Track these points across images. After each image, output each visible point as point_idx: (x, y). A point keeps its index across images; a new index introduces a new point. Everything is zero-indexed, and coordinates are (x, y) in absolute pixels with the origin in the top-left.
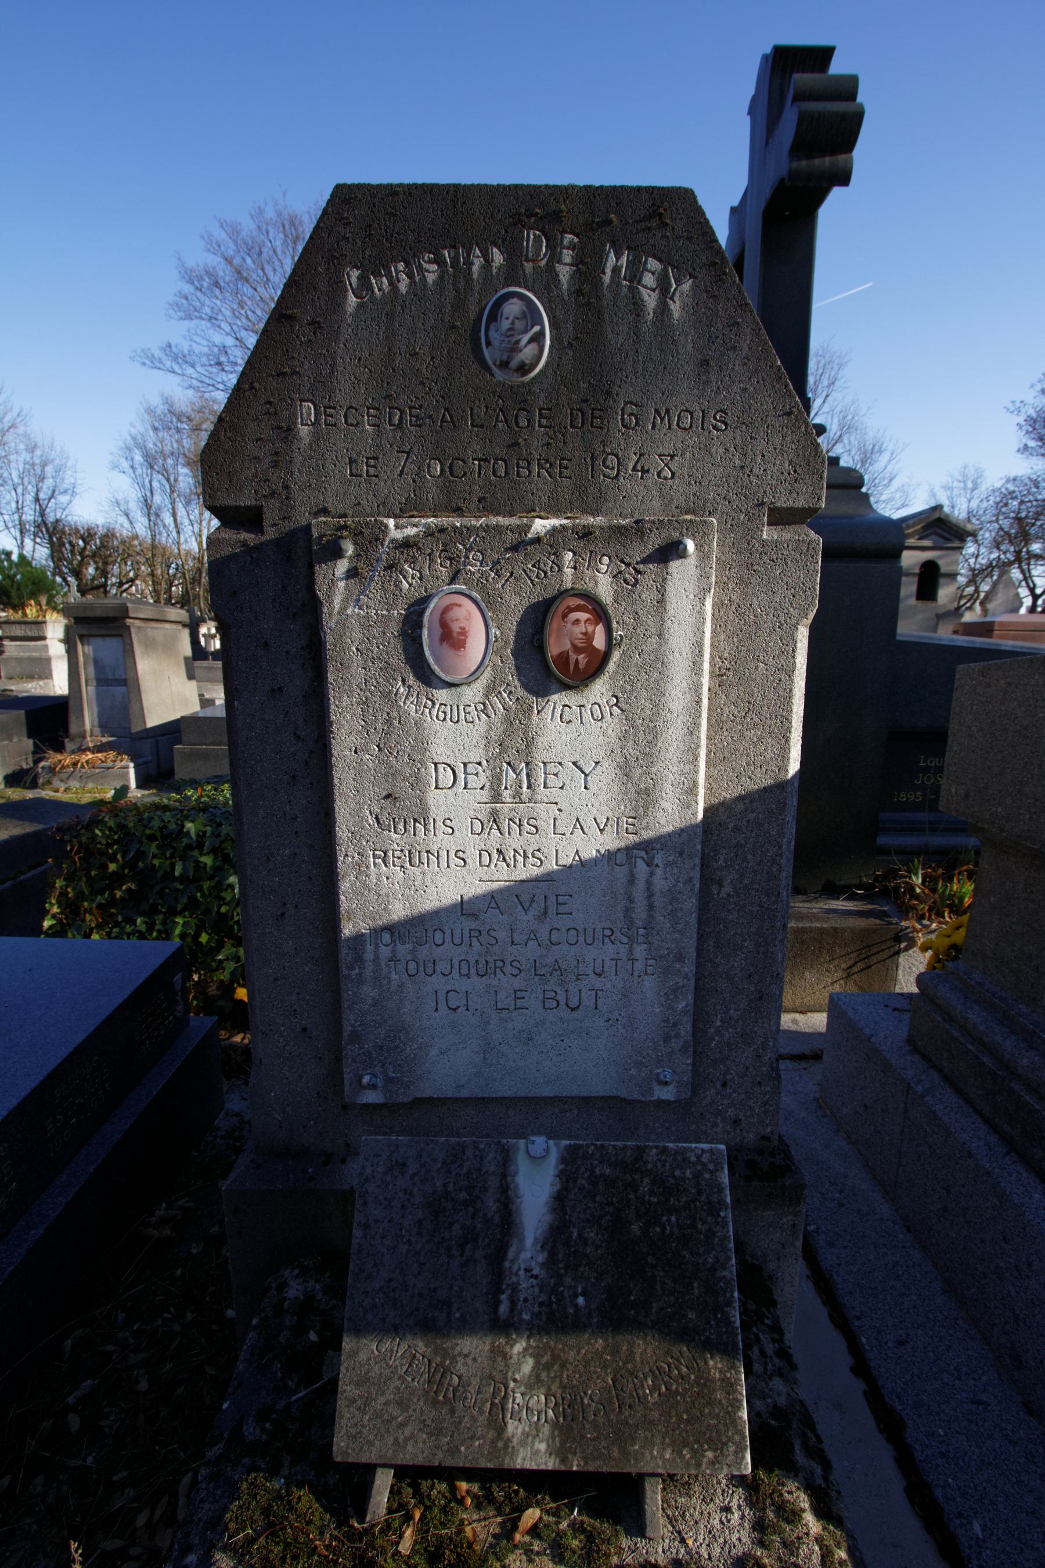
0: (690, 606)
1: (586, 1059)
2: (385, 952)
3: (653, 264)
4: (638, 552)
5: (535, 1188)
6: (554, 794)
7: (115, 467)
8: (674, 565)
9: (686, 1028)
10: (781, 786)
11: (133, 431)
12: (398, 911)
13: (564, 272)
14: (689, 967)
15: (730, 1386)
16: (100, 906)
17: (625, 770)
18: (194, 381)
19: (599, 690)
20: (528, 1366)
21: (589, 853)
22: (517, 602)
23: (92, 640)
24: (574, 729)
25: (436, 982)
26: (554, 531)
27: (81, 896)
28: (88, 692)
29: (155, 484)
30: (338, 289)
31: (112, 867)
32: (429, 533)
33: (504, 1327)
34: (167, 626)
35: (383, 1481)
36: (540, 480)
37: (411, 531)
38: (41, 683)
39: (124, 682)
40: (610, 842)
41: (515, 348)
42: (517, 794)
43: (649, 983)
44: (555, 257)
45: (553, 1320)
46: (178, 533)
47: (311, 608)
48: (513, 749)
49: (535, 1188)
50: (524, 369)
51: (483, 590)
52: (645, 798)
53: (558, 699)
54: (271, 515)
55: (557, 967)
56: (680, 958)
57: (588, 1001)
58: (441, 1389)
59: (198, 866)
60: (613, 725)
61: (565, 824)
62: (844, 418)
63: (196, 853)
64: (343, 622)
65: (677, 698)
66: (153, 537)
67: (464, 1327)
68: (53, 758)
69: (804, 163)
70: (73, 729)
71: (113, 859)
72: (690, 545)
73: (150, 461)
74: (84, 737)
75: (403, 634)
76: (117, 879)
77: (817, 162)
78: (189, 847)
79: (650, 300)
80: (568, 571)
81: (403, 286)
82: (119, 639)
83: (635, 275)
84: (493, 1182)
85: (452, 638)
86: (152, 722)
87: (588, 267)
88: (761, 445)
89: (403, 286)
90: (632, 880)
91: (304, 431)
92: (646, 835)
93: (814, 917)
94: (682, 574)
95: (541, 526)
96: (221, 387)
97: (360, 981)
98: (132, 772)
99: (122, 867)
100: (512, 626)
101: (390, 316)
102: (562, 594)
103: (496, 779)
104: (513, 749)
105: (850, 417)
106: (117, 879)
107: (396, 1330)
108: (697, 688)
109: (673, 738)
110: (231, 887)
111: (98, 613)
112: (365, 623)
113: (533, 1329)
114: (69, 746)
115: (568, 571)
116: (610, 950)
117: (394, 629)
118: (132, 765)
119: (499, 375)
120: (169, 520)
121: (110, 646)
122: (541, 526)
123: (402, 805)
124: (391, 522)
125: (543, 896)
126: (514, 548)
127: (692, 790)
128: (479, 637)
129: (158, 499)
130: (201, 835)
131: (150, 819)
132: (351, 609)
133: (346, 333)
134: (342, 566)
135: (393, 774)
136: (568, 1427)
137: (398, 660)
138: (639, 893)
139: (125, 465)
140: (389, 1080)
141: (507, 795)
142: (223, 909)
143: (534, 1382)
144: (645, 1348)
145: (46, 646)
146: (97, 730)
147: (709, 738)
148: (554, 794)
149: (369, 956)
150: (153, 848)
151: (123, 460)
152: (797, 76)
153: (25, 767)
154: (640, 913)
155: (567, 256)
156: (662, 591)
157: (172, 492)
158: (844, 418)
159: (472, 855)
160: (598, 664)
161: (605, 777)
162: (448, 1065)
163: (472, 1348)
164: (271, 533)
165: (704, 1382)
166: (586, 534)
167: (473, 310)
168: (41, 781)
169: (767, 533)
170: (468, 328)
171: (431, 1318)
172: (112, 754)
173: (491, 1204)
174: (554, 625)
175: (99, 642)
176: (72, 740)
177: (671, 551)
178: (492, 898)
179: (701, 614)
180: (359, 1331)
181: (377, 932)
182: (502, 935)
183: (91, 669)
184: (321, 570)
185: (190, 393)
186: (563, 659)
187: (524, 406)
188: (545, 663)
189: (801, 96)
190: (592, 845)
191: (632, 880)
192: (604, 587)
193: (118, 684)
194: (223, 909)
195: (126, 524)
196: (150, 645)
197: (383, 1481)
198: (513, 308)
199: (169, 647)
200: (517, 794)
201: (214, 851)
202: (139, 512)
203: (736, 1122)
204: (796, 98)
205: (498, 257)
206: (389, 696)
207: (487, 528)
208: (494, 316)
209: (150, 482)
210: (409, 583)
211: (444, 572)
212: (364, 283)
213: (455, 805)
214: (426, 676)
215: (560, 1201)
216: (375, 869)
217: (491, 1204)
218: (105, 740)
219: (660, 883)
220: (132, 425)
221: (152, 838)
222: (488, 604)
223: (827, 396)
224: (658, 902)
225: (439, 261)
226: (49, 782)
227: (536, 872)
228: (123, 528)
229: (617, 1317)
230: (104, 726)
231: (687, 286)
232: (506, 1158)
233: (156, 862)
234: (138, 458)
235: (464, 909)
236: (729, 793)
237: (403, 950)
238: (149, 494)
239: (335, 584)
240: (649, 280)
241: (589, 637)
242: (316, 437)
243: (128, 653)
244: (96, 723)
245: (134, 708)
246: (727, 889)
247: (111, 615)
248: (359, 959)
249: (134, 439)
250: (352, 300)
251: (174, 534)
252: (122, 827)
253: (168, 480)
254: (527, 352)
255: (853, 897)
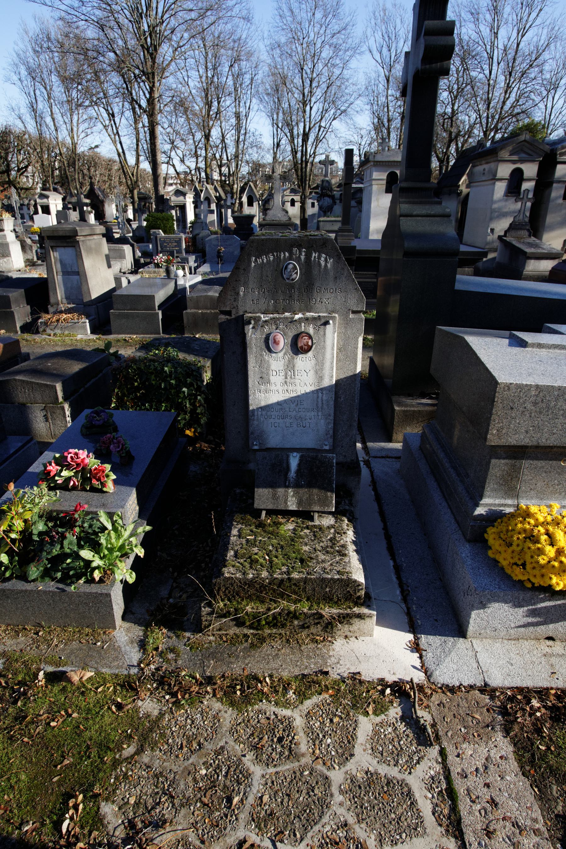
0: (332, 336)
1: (309, 440)
2: (260, 413)
3: (324, 255)
4: (319, 323)
5: (294, 462)
6: (300, 377)
7: (8, 79)
8: (327, 326)
9: (331, 432)
10: (355, 376)
11: (16, 48)
12: (263, 404)
13: (303, 257)
14: (332, 418)
15: (332, 497)
16: (132, 399)
17: (316, 372)
18: (63, 14)
19: (310, 354)
20: (292, 493)
21: (308, 391)
22: (291, 334)
23: (58, 249)
24: (304, 362)
25: (272, 420)
26: (300, 319)
27: (124, 395)
28: (58, 279)
29: (38, 92)
30: (250, 262)
31: (136, 384)
32: (271, 319)
33: (288, 487)
34: (95, 237)
35: (264, 513)
36: (297, 304)
37: (267, 318)
38: (5, 260)
39: (78, 273)
40: (313, 388)
41: (291, 275)
42: (291, 377)
43: (322, 421)
44: (300, 254)
45: (297, 485)
46: (56, 130)
47: (244, 335)
48: (290, 367)
49: (294, 462)
50: (293, 280)
51: (283, 332)
52: (321, 378)
53: (301, 356)
54: (234, 312)
55: (300, 417)
56: (330, 415)
57: (308, 425)
58: (275, 497)
59: (171, 384)
60: (313, 362)
61: (302, 384)
62: (553, 29)
63: (168, 379)
64: (251, 339)
65: (328, 355)
66: (40, 134)
67: (279, 487)
68: (45, 317)
69: (428, 66)
70: (52, 300)
71: (136, 381)
72: (331, 322)
73: (31, 72)
74: (58, 304)
75: (265, 341)
76: (138, 389)
77: (434, 65)
78: (167, 377)
79: (323, 263)
80: (303, 327)
81: (265, 261)
82: (73, 248)
83: (319, 258)
84: (285, 461)
85: (276, 342)
86: (94, 295)
87: (308, 256)
88: (349, 296)
89: (265, 261)
90: (318, 397)
91: (241, 293)
92: (321, 387)
93: (413, 406)
94: (329, 328)
95: (297, 317)
96: (83, 17)
97: (254, 420)
98: (88, 324)
99: (139, 384)
100: (290, 340)
101: (262, 268)
102: (302, 332)
103: (286, 374)
104: (290, 367)
105: (556, 28)
106: (138, 389)
107: (266, 487)
108: (333, 354)
109: (327, 365)
110: (184, 392)
111: (61, 234)
112: (256, 339)
113: (293, 487)
114: (51, 310)
115: (303, 327)
116: (313, 413)
117: (263, 340)
118: (87, 321)
119: (287, 281)
120: (48, 120)
121: (69, 252)
122: (297, 317)
123: (264, 379)
124: (262, 316)
125: (297, 401)
126: (291, 322)
127: (332, 377)
128: (283, 342)
129: (40, 106)
130: (171, 372)
131: (150, 366)
132: (253, 336)
133: (252, 272)
134: (251, 326)
135: (262, 372)
136: (300, 503)
137: (264, 347)
138: (320, 400)
139: (15, 78)
140: (260, 444)
141: (289, 377)
142: (180, 401)
143: (293, 496)
144: (315, 491)
145: (5, 235)
146: (65, 301)
147: (337, 364)
148: (300, 377)
149: (256, 414)
150: (153, 377)
151: (13, 74)
152: (426, 22)
153: (28, 321)
154: (320, 405)
155: (303, 254)
156: (325, 332)
157: (49, 98)
158: (553, 29)
159: (280, 391)
160: (309, 349)
161: (312, 373)
162: (274, 440)
163: (281, 491)
164: (233, 316)
165: (327, 497)
166: (307, 319)
167: (281, 266)
168: (41, 330)
169: (351, 316)
170: (280, 270)
171: (273, 485)
172: (76, 315)
173: (285, 465)
174: (300, 340)
175: (62, 249)
176: (52, 306)
177: (326, 323)
178: (285, 401)
179: (334, 337)
180: (258, 487)
181: (258, 409)
182: (287, 409)
183: (59, 266)
184: (246, 327)
185: (60, 23)
186: (302, 347)
187: (293, 287)
188: (298, 347)
189: (428, 33)
190: (309, 389)
191: (318, 397)
192: (311, 331)
193: (75, 274)
194: (180, 401)
195: (21, 125)
196: (90, 251)
197: (264, 513)
198: (291, 266)
199: (98, 250)
200: (291, 377)
201: (175, 379)
202: (28, 115)
203: (345, 456)
204: (425, 35)
205: (287, 254)
206: (262, 355)
207: (284, 318)
208: (286, 268)
209: (34, 91)
210: (266, 330)
211: (274, 327)
212: (256, 260)
213: (276, 379)
214: (270, 350)
215: (299, 465)
216: (258, 394)
217: (285, 465)
218: (70, 306)
219: (324, 398)
220: (15, 43)
221: (152, 373)
222: (285, 335)
223: (541, 10)
224: (324, 402)
225: (273, 255)
226: (44, 331)
227: (295, 395)
228: (18, 127)
229: (310, 485)
230: (69, 298)
231: (331, 260)
232: (288, 457)
233: (154, 382)
234: (24, 72)
235: (278, 403)
236: (342, 376)
237: (264, 413)
238: (34, 101)
239: (249, 329)
240: (323, 259)
241: (308, 342)
242: (244, 295)
243: (79, 256)
244: (64, 296)
245: (84, 288)
246: (342, 399)
247: (68, 234)
248: (253, 415)
249: (18, 55)
250: (253, 264)
251: (54, 132)
252: (139, 369)
253: (46, 88)
254: (294, 276)
255: (431, 398)
